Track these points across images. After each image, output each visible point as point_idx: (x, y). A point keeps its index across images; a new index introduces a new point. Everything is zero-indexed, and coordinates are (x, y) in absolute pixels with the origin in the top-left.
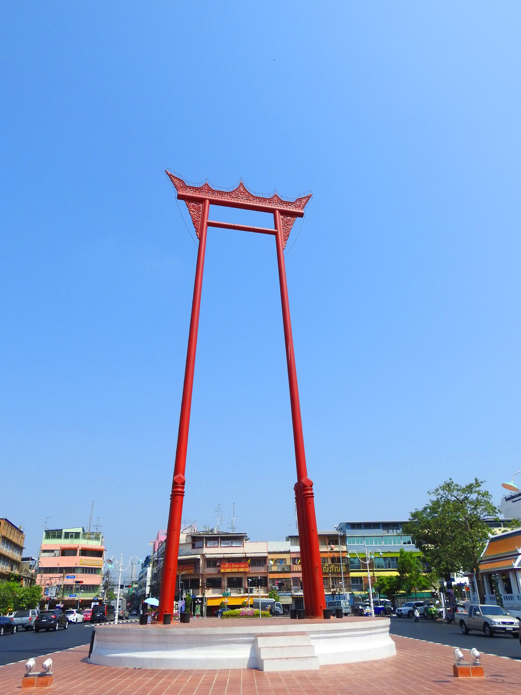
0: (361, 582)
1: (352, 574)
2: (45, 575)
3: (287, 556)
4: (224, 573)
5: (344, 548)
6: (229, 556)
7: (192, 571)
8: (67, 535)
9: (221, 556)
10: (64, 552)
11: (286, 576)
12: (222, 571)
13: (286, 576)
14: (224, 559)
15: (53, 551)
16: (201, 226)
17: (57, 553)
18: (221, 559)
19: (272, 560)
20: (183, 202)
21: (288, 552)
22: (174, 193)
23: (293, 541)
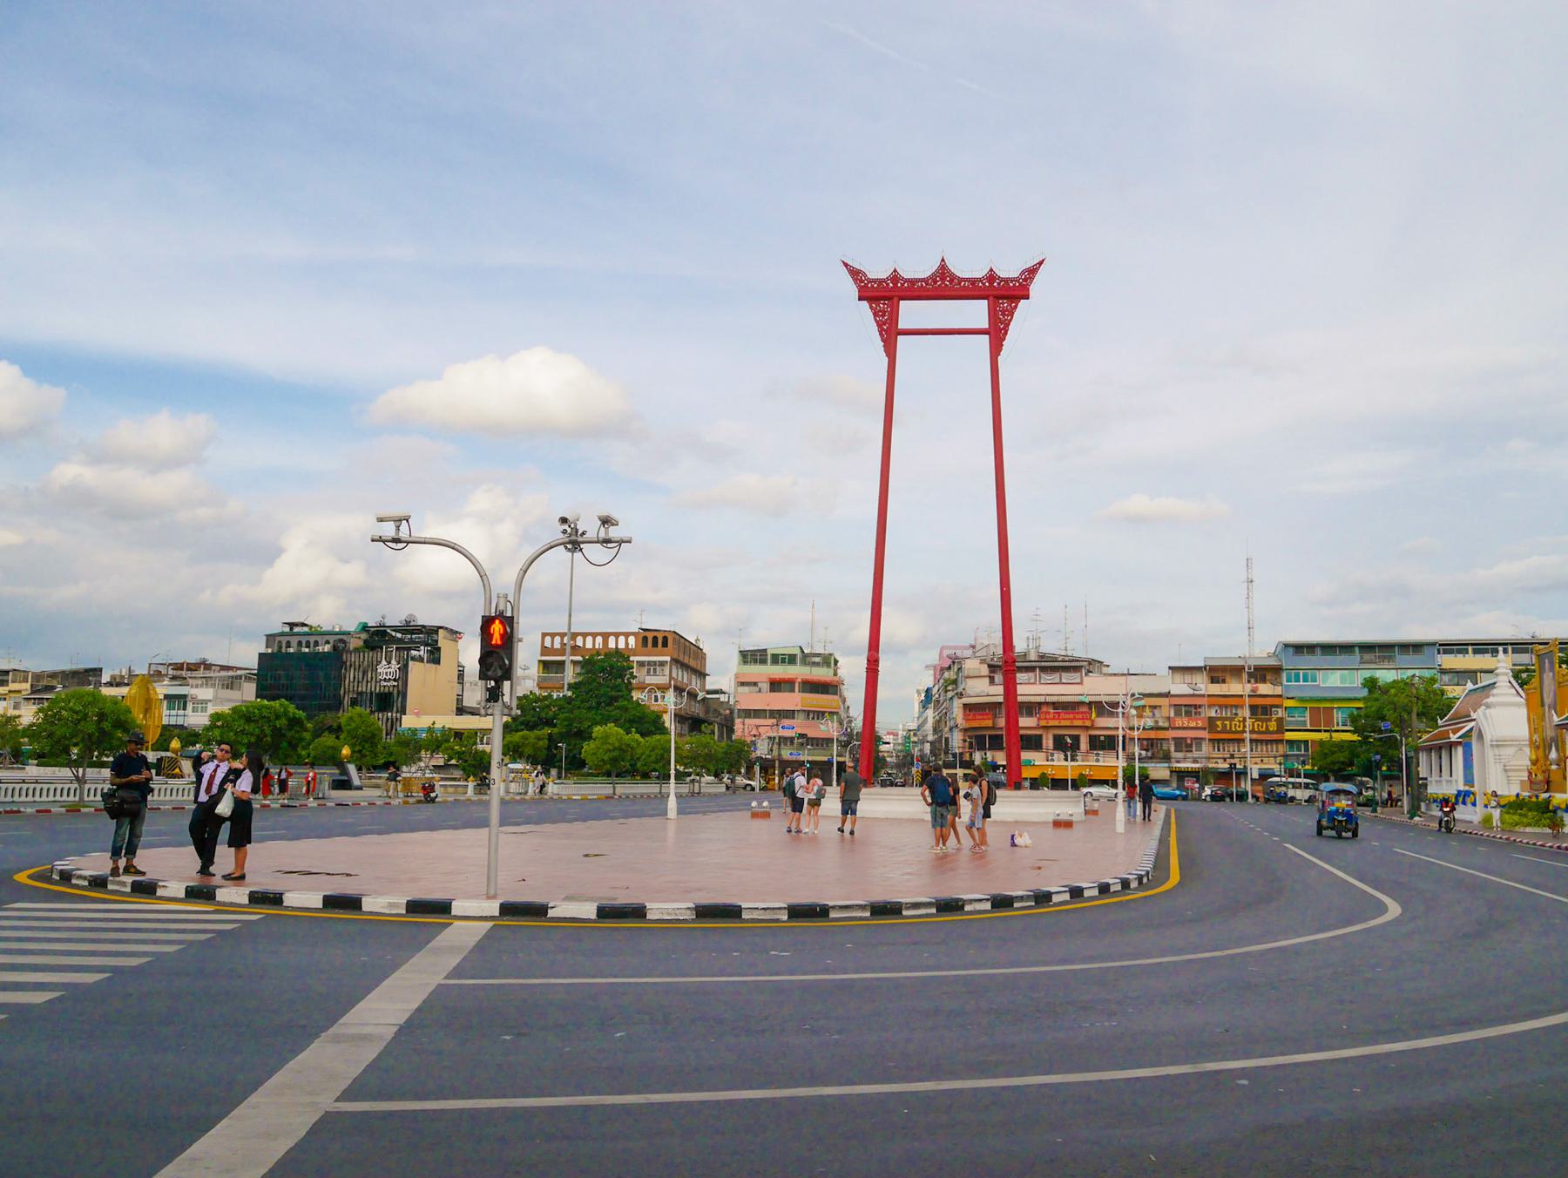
0: (1307, 750)
1: (1289, 736)
2: (747, 721)
3: (1164, 701)
4: (1046, 728)
5: (1278, 690)
6: (1055, 699)
7: (989, 723)
8: (776, 659)
9: (1041, 699)
10: (776, 685)
11: (1161, 734)
12: (1043, 723)
13: (1161, 734)
14: (1047, 703)
15: (755, 684)
16: (890, 333)
17: (765, 686)
18: (1040, 704)
19: (1137, 708)
20: (865, 304)
21: (1167, 695)
22: (854, 291)
23: (1178, 677)
